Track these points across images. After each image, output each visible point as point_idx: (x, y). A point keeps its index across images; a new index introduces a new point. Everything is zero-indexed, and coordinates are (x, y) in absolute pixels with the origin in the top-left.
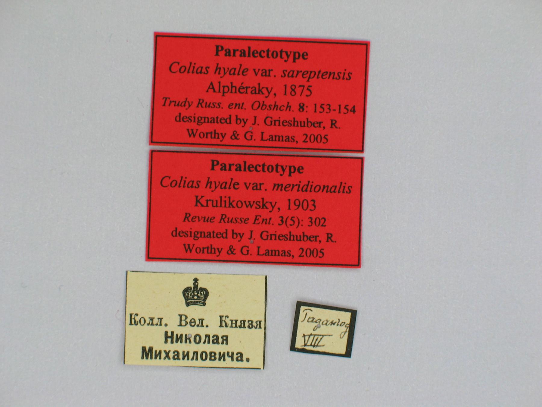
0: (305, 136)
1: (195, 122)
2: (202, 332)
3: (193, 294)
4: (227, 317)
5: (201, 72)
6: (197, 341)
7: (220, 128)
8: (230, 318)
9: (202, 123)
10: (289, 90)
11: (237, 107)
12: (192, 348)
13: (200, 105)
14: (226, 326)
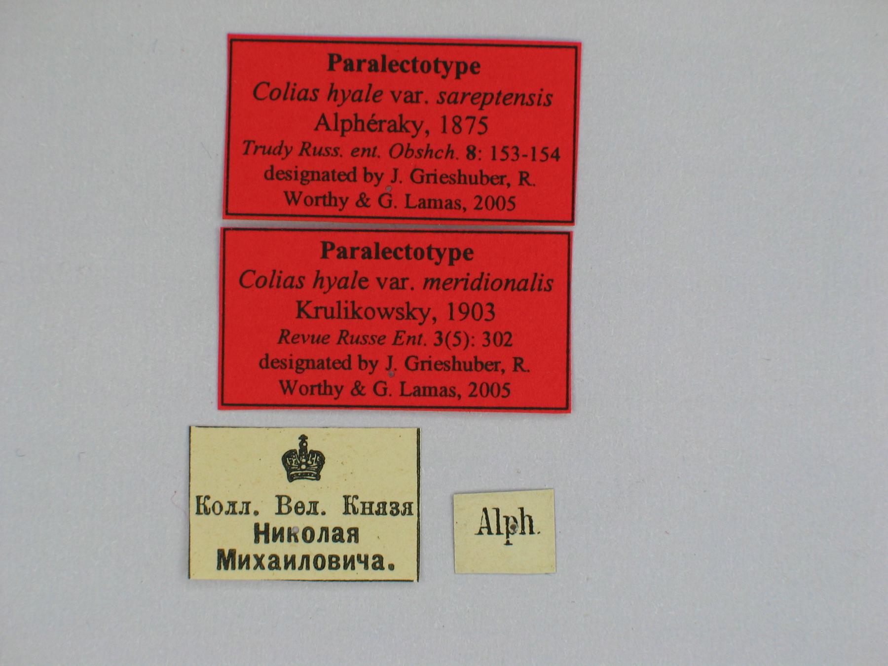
0: (478, 200)
1: (298, 180)
2: (316, 522)
3: (299, 462)
4: (357, 497)
5: (305, 99)
6: (308, 538)
7: (338, 189)
8: (361, 499)
9: (309, 181)
10: (450, 124)
11: (366, 154)
12: (299, 549)
13: (304, 152)
14: (355, 512)
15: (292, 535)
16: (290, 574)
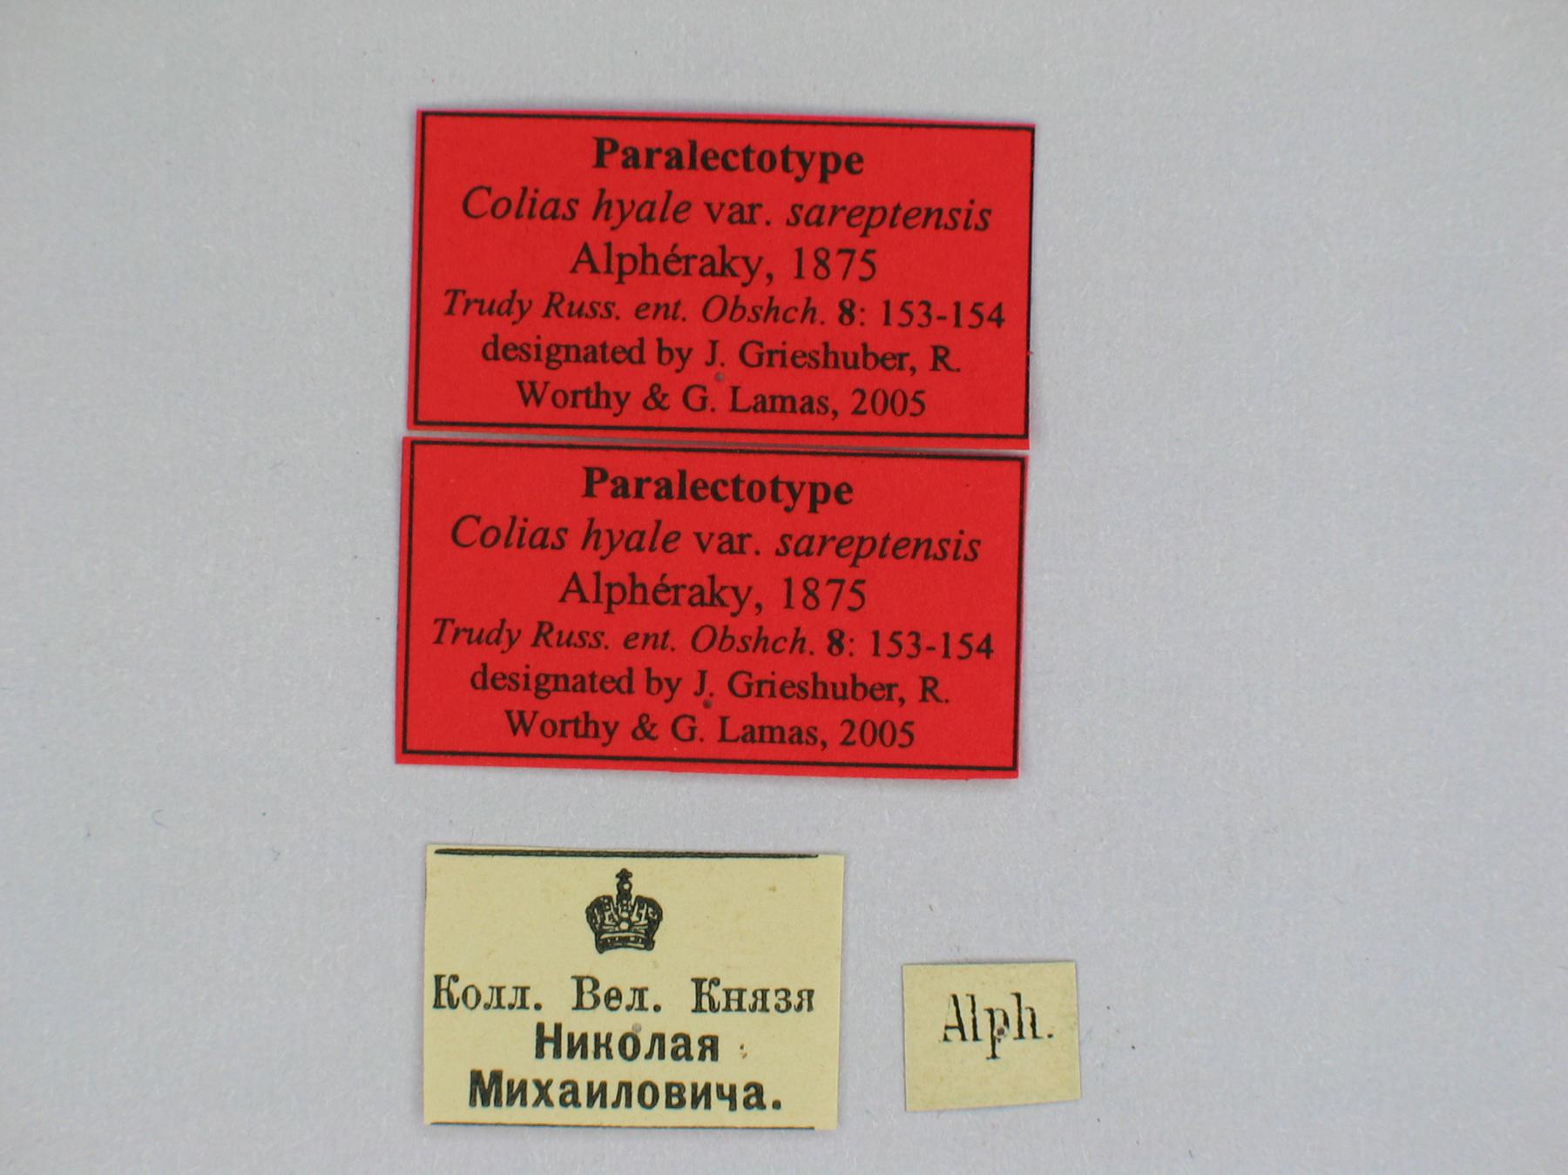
6: (629, 1051)
12: (612, 1071)
15: (602, 1045)
16: (596, 1115)
